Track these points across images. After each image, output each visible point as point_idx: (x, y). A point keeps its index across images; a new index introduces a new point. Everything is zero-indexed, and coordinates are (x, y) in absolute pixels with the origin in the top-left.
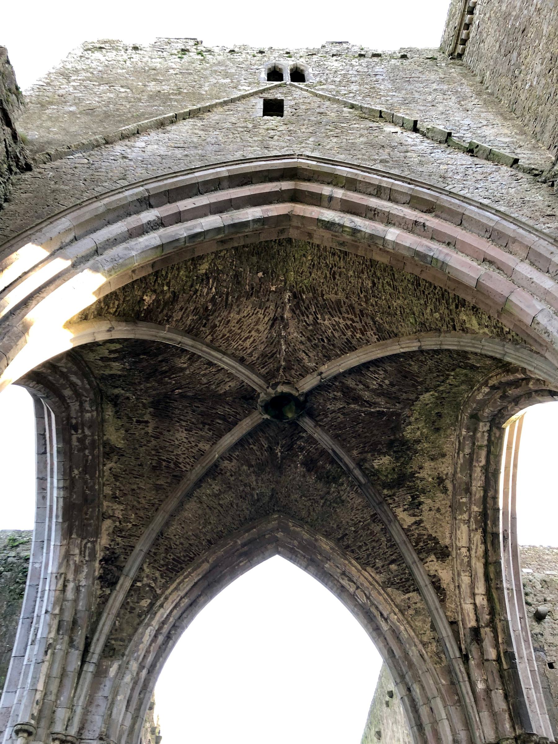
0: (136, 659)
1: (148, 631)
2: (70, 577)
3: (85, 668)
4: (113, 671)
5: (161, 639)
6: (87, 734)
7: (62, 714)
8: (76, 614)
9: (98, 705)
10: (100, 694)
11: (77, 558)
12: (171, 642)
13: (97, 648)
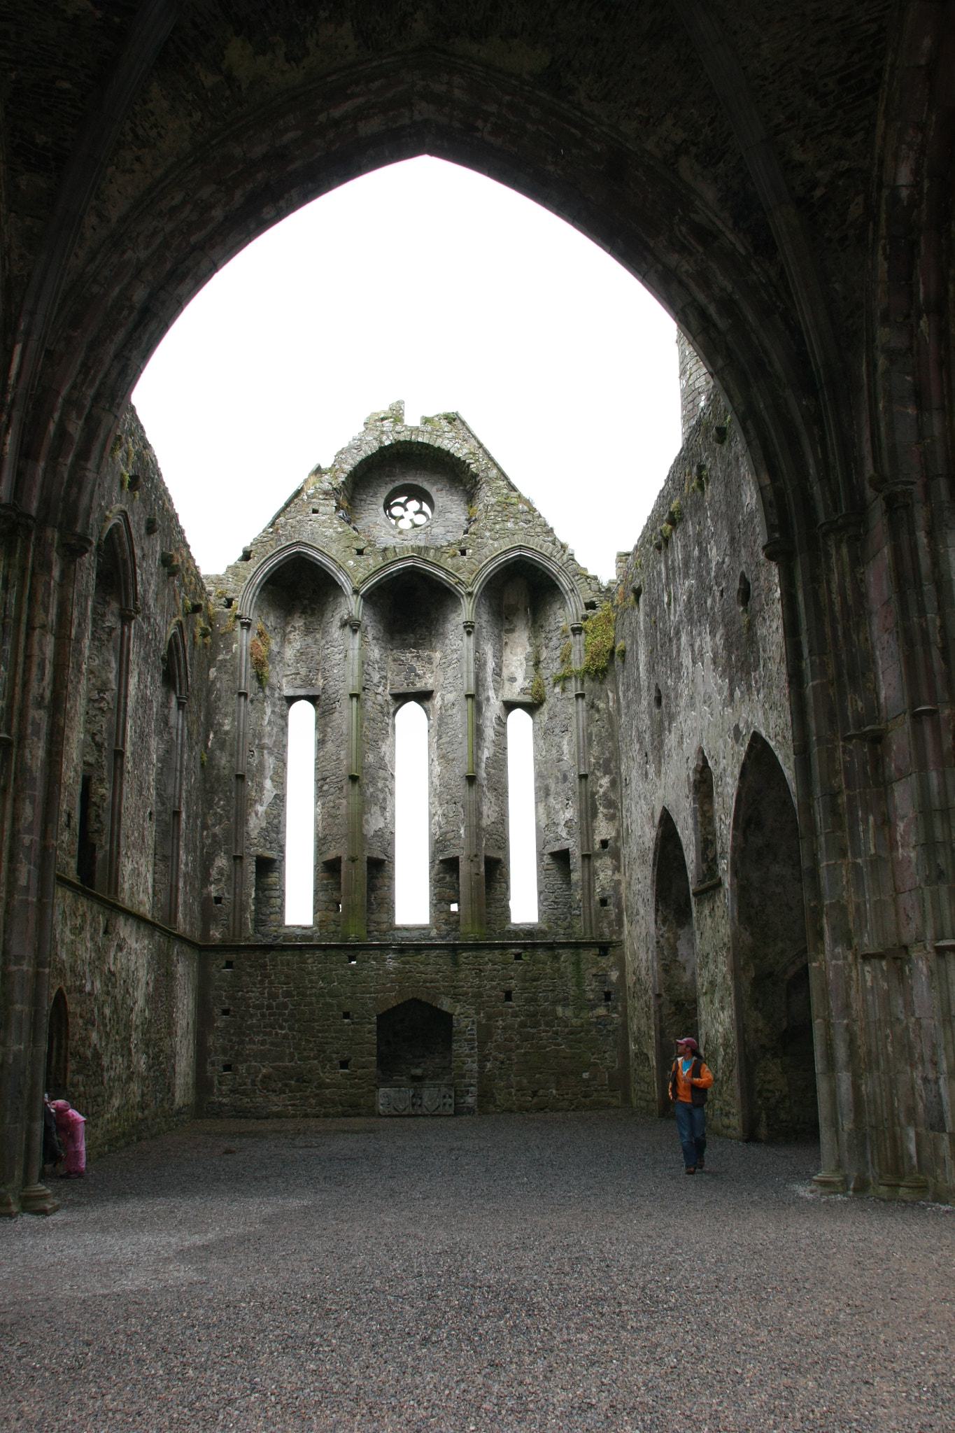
2: (701, 297)
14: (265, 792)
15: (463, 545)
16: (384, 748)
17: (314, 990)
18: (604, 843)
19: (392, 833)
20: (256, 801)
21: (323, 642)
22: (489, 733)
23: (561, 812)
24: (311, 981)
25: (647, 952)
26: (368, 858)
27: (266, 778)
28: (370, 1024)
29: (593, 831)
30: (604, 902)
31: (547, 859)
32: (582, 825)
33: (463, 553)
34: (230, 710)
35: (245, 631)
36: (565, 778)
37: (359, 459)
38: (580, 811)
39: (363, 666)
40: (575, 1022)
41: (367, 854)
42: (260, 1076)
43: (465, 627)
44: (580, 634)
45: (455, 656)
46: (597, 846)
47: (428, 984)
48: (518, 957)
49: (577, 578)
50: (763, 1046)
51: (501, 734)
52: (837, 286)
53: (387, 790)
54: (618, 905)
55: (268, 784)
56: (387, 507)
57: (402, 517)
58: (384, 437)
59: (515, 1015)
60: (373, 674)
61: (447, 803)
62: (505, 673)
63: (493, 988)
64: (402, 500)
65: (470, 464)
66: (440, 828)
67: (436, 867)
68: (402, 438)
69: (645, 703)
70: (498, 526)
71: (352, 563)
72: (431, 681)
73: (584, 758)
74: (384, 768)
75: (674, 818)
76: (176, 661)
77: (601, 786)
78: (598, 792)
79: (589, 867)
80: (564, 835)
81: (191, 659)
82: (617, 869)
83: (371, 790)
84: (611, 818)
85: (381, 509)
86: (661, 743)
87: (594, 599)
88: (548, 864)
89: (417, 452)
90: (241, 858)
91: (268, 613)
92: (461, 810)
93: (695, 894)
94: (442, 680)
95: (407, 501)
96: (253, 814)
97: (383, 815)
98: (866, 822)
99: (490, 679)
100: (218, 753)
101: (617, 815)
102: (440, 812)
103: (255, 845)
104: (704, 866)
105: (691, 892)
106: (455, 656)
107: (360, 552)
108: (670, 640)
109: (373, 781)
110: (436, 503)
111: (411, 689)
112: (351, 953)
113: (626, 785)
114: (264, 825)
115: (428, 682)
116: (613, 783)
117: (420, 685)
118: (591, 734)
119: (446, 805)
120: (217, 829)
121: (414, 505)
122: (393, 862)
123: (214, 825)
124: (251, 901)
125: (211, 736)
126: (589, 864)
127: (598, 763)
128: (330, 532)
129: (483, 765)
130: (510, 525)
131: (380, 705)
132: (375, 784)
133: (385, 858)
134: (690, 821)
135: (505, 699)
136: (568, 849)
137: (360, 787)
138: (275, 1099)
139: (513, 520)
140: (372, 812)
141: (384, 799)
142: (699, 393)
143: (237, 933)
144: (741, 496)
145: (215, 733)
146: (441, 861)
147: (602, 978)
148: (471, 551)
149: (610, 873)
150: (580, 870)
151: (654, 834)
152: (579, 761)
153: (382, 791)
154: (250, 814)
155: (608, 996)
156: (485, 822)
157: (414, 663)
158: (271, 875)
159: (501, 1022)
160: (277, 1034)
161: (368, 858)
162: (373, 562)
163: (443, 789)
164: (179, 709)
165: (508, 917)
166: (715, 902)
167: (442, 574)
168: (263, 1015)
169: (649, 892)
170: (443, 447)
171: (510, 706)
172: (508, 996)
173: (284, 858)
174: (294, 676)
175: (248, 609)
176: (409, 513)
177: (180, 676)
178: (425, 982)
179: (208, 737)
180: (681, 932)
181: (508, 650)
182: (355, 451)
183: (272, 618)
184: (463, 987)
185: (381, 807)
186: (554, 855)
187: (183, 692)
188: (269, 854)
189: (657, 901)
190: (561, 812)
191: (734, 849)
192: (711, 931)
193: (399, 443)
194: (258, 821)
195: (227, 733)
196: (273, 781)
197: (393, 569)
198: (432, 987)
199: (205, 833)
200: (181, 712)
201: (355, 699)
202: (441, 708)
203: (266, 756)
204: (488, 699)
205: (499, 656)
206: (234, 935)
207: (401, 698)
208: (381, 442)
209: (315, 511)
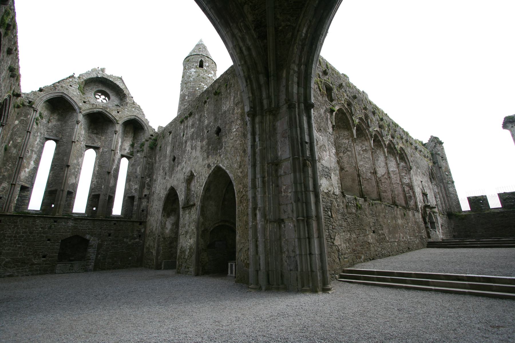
0: (294, 62)
1: (295, 47)
2: (241, 44)
3: (270, 80)
4: (284, 75)
5: (306, 49)
6: (281, 104)
7: (265, 102)
8: (254, 60)
9: (282, 91)
10: (282, 86)
11: (239, 34)
12: (314, 46)
13: (272, 68)
14: (30, 165)
15: (118, 110)
16: (80, 160)
17: (37, 232)
18: (145, 195)
19: (77, 185)
20: (26, 167)
21: (64, 125)
22: (116, 162)
24: (36, 228)
25: (157, 224)
26: (68, 191)
27: (32, 161)
28: (58, 243)
29: (143, 192)
30: (143, 211)
31: (126, 198)
32: (140, 190)
33: (118, 112)
36: (137, 177)
38: (140, 186)
40: (130, 243)
41: (68, 189)
42: (4, 262)
43: (115, 132)
45: (110, 139)
46: (143, 196)
47: (83, 231)
48: (115, 224)
50: (203, 249)
52: (278, 53)
54: (147, 212)
55: (32, 163)
56: (95, 95)
57: (99, 99)
59: (111, 241)
60: (81, 137)
62: (123, 147)
63: (105, 232)
64: (100, 94)
65: (124, 91)
66: (95, 185)
69: (167, 160)
72: (100, 144)
74: (79, 165)
75: (176, 189)
77: (147, 181)
79: (140, 201)
80: (134, 192)
81: (10, 112)
82: (148, 202)
83: (73, 171)
84: (148, 189)
85: (93, 94)
86: (173, 170)
90: (15, 185)
91: (45, 110)
92: (104, 181)
93: (183, 208)
94: (103, 145)
95: (101, 95)
96: (24, 171)
98: (272, 185)
99: (119, 148)
100: (13, 148)
103: (22, 181)
104: (186, 201)
105: (181, 207)
106: (110, 139)
107: (85, 102)
108: (182, 144)
111: (93, 145)
112: (55, 220)
113: (155, 181)
115: (99, 144)
116: (150, 180)
118: (146, 167)
121: (103, 97)
124: (15, 200)
125: (11, 142)
128: (75, 93)
129: (113, 170)
130: (133, 109)
134: (184, 189)
135: (122, 154)
138: (9, 270)
141: (77, 175)
143: (6, 210)
144: (221, 107)
145: (13, 142)
146: (93, 195)
147: (139, 231)
149: (146, 203)
151: (166, 193)
153: (77, 172)
154: (22, 171)
155: (140, 236)
156: (111, 185)
157: (95, 138)
158: (26, 192)
159: (106, 243)
160: (16, 246)
161: (68, 191)
162: (87, 106)
163: (98, 174)
165: (112, 213)
166: (191, 209)
167: (110, 116)
168: (11, 240)
171: (123, 156)
172: (110, 235)
176: (101, 99)
177: (4, 115)
178: (82, 230)
179: (9, 142)
180: (168, 219)
181: (125, 141)
183: (46, 112)
184: (95, 232)
185: (75, 177)
186: (129, 197)
187: (4, 122)
189: (163, 211)
190: (134, 186)
191: (202, 196)
192: (188, 218)
193: (103, 78)
194: (25, 174)
195: (19, 143)
198: (84, 232)
202: (102, 152)
204: (117, 153)
205: (122, 142)
206: (4, 211)
207: (88, 147)
209: (71, 86)
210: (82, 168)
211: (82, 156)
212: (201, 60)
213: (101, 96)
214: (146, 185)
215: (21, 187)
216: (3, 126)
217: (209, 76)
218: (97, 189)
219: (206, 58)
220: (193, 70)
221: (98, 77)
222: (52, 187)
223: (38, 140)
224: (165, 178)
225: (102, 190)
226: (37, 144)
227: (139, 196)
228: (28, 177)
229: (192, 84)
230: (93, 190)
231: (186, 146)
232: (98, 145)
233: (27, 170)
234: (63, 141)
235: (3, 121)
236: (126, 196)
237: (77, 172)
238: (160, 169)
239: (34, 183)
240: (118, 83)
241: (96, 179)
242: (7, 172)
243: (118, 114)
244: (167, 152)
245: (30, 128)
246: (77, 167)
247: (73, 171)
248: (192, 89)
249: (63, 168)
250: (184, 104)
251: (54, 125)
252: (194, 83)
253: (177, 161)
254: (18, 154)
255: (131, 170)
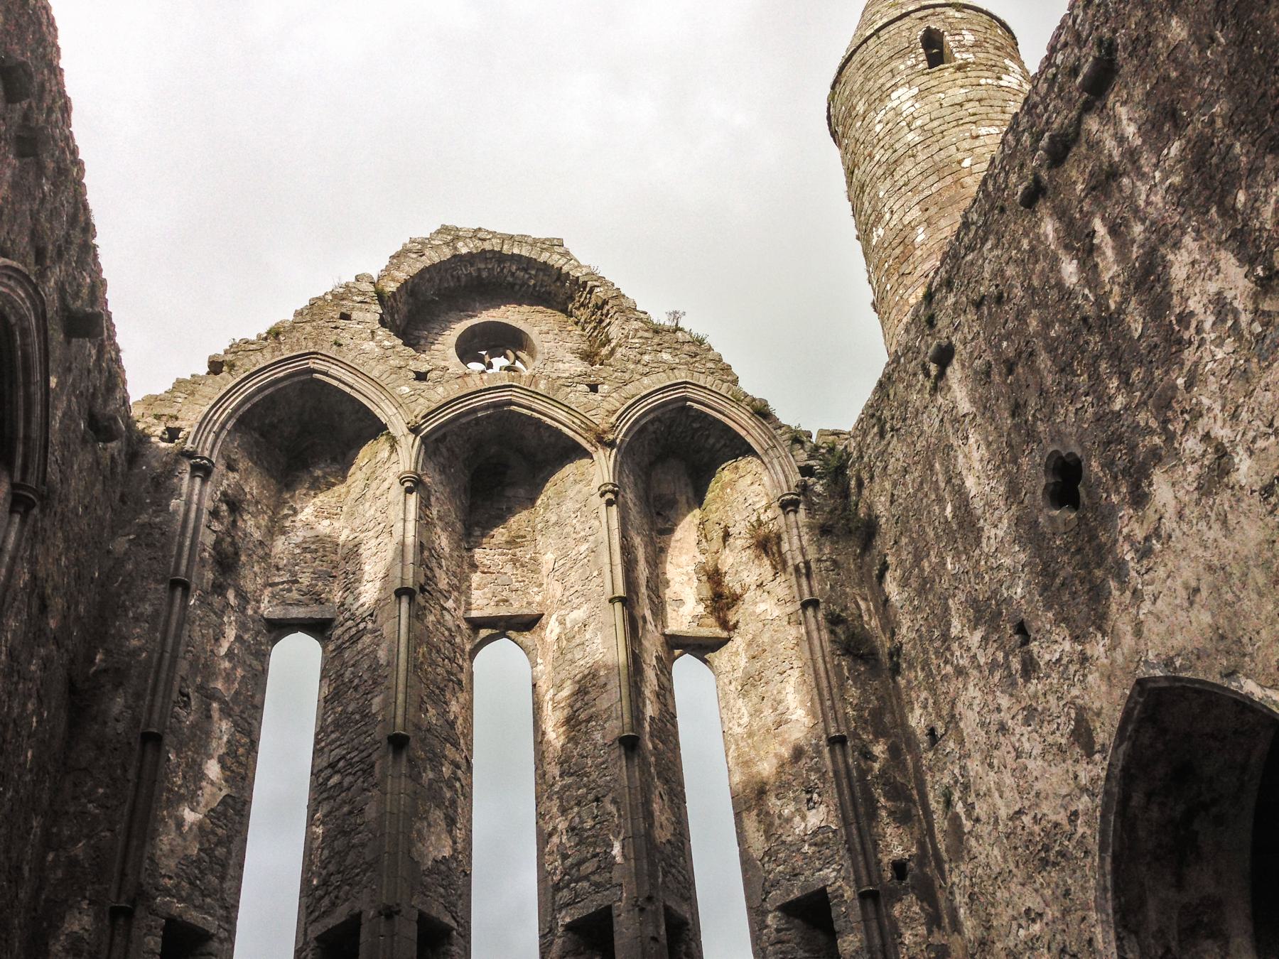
16: (454, 707)
18: (899, 868)
20: (181, 799)
22: (650, 674)
23: (797, 819)
27: (210, 757)
29: (876, 844)
32: (849, 834)
33: (594, 388)
34: (147, 608)
35: (198, 480)
37: (420, 266)
38: (842, 806)
39: (422, 552)
43: (602, 495)
44: (796, 512)
45: (583, 548)
46: (888, 875)
49: (780, 432)
51: (665, 692)
53: (458, 785)
55: (213, 769)
58: (460, 244)
60: (437, 572)
61: (578, 804)
66: (565, 857)
67: (559, 941)
68: (487, 246)
70: (646, 358)
71: (408, 390)
73: (833, 707)
74: (456, 745)
76: (21, 403)
78: (871, 769)
82: (934, 921)
83: (431, 775)
84: (903, 818)
87: (812, 463)
88: (778, 931)
89: (510, 279)
92: (612, 808)
97: (450, 832)
101: (914, 812)
102: (562, 826)
103: (167, 892)
106: (583, 548)
107: (421, 377)
109: (436, 760)
110: (539, 348)
114: (194, 850)
116: (894, 751)
117: (516, 607)
119: (576, 810)
120: (79, 849)
122: (466, 936)
123: (74, 840)
126: (877, 911)
127: (861, 717)
130: (666, 356)
131: (449, 630)
132: (437, 768)
133: (454, 924)
135: (667, 631)
136: (824, 889)
137: (409, 761)
139: (670, 350)
140: (431, 819)
141: (453, 802)
142: (913, 229)
146: (569, 928)
148: (606, 387)
149: (922, 930)
150: (862, 926)
151: (1093, 771)
152: (824, 714)
163: (568, 780)
164: (12, 512)
167: (561, 415)
169: (1093, 916)
170: (551, 262)
173: (232, 933)
174: (286, 586)
175: (208, 445)
182: (414, 256)
185: (447, 816)
186: (789, 909)
188: (194, 917)
189: (1119, 938)
190: (797, 819)
194: (179, 840)
195: (135, 652)
196: (224, 767)
197: (476, 402)
199: (50, 857)
200: (17, 519)
201: (405, 600)
203: (216, 715)
208: (456, 248)
209: (345, 317)
210: (475, 761)
211: (460, 682)
212: (928, 27)
213: (494, 361)
214: (878, 792)
215: (164, 929)
216: (29, 505)
217: (1002, 83)
218: (586, 878)
219: (951, 12)
220: (903, 97)
221: (461, 256)
222: (333, 904)
223: (231, 633)
224: (1030, 667)
225: (616, 874)
226: (230, 655)
227: (857, 881)
228: (200, 860)
229: (921, 157)
230: (565, 895)
231: (1158, 307)
232: (529, 603)
233: (190, 816)
234: (353, 617)
235: (23, 479)
236: (768, 906)
237: (452, 787)
238: (945, 637)
239: (235, 907)
240: (556, 257)
241: (564, 811)
242: (89, 837)
243: (598, 397)
244: (970, 482)
245: (184, 562)
246: (449, 751)
247: (431, 775)
248: (934, 178)
249: (373, 766)
250: (918, 272)
251: (297, 546)
252: (935, 148)
253: (1108, 464)
254: (136, 721)
255: (745, 720)
